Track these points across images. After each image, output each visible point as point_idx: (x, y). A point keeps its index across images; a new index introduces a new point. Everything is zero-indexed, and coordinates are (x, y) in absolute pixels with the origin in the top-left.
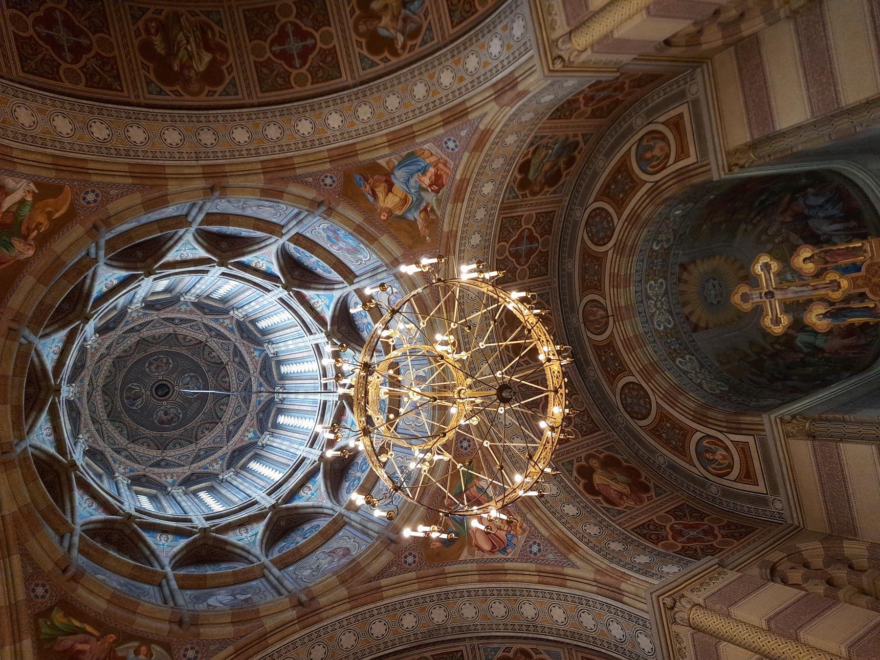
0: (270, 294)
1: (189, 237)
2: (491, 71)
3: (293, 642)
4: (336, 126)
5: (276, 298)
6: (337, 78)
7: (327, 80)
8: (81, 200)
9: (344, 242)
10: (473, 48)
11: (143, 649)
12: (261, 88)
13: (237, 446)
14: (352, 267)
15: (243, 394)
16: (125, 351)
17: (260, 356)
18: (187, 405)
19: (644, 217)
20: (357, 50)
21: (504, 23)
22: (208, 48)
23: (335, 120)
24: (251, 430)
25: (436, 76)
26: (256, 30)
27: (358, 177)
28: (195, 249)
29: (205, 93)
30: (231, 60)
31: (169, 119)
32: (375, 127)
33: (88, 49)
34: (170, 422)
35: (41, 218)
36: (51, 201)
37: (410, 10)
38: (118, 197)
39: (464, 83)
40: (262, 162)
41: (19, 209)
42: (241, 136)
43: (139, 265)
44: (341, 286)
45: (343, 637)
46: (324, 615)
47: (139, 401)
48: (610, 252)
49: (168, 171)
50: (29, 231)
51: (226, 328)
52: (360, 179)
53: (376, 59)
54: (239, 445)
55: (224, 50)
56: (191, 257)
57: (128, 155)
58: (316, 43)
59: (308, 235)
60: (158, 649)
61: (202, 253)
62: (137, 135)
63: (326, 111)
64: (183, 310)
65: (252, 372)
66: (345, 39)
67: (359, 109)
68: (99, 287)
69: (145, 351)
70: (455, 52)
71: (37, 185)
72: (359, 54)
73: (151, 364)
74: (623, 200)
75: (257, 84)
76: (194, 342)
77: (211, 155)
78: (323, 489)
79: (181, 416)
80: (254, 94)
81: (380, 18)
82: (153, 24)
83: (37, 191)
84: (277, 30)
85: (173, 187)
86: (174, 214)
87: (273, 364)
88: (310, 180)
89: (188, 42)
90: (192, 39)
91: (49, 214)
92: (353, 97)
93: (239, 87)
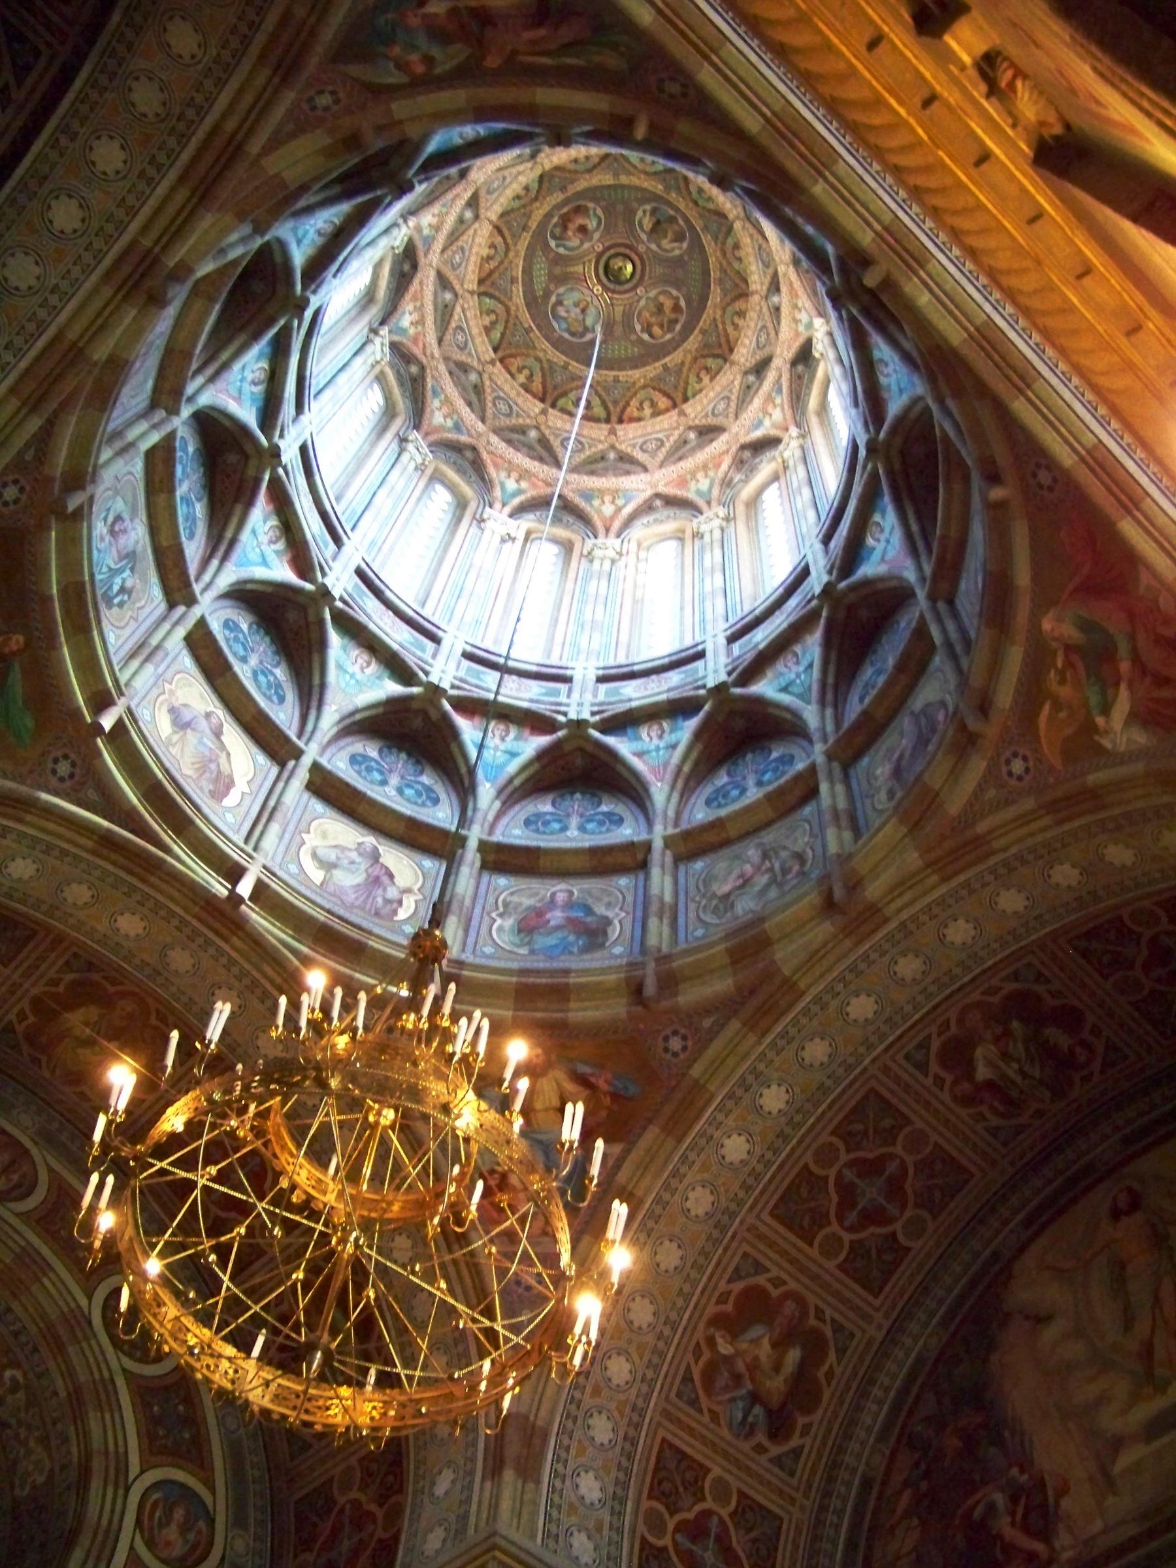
0: (592, 675)
1: (811, 715)
2: (568, 1449)
3: (133, 212)
4: (727, 1142)
5: (577, 676)
6: (776, 1206)
7: (788, 1189)
8: (1028, 753)
9: (558, 928)
10: (618, 1449)
11: (420, 69)
12: (877, 1094)
13: (416, 281)
14: (502, 881)
15: (473, 377)
16: (741, 314)
17: (502, 485)
18: (557, 270)
19: (91, 1414)
20: (775, 1272)
21: (606, 1532)
22: (990, 1085)
23: (736, 1147)
24: (412, 331)
25: (635, 1357)
26: (938, 1166)
27: (633, 1090)
28: (784, 689)
29: (953, 1024)
30: (946, 1096)
31: (981, 953)
32: (666, 1196)
33: (1146, 967)
34: (565, 222)
35: (1065, 692)
36: (1069, 731)
37: (742, 1398)
38: (980, 789)
39: (588, 1390)
40: (803, 993)
41: (1103, 693)
42: (862, 1007)
43: (852, 597)
44: (490, 817)
45: (37, 271)
46: (107, 292)
47: (647, 223)
48: (83, 1302)
49: (935, 878)
50: (1069, 664)
51: (601, 493)
52: (626, 1088)
53: (738, 1287)
54: (414, 287)
55: (967, 1101)
56: (780, 666)
57: (1006, 864)
58: (841, 1225)
59: (623, 881)
60: (391, 80)
61: (765, 688)
62: (1011, 901)
63: (758, 1151)
64: (700, 475)
65: (494, 439)
66: (803, 1270)
67: (711, 1198)
68: (887, 519)
69: (703, 332)
70: (636, 1418)
71: (1100, 750)
72: (768, 1270)
73: (676, 308)
74: (147, 1405)
75: (887, 1095)
76: (632, 410)
77: (886, 946)
78: (233, 408)
79: (553, 244)
80: (880, 1076)
81: (775, 1345)
82: (1082, 1059)
83: (1096, 738)
84: (909, 1190)
85: (913, 859)
86: (865, 761)
87: (467, 490)
88: (707, 1023)
89: (1022, 1072)
90: (1018, 1079)
91: (1057, 706)
92: (733, 1206)
93: (912, 1070)
